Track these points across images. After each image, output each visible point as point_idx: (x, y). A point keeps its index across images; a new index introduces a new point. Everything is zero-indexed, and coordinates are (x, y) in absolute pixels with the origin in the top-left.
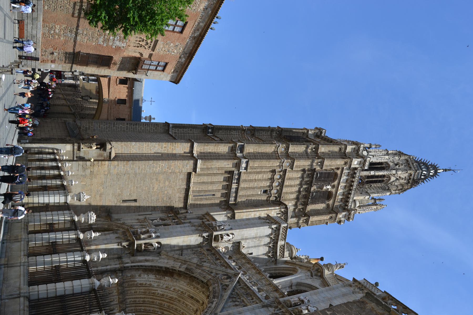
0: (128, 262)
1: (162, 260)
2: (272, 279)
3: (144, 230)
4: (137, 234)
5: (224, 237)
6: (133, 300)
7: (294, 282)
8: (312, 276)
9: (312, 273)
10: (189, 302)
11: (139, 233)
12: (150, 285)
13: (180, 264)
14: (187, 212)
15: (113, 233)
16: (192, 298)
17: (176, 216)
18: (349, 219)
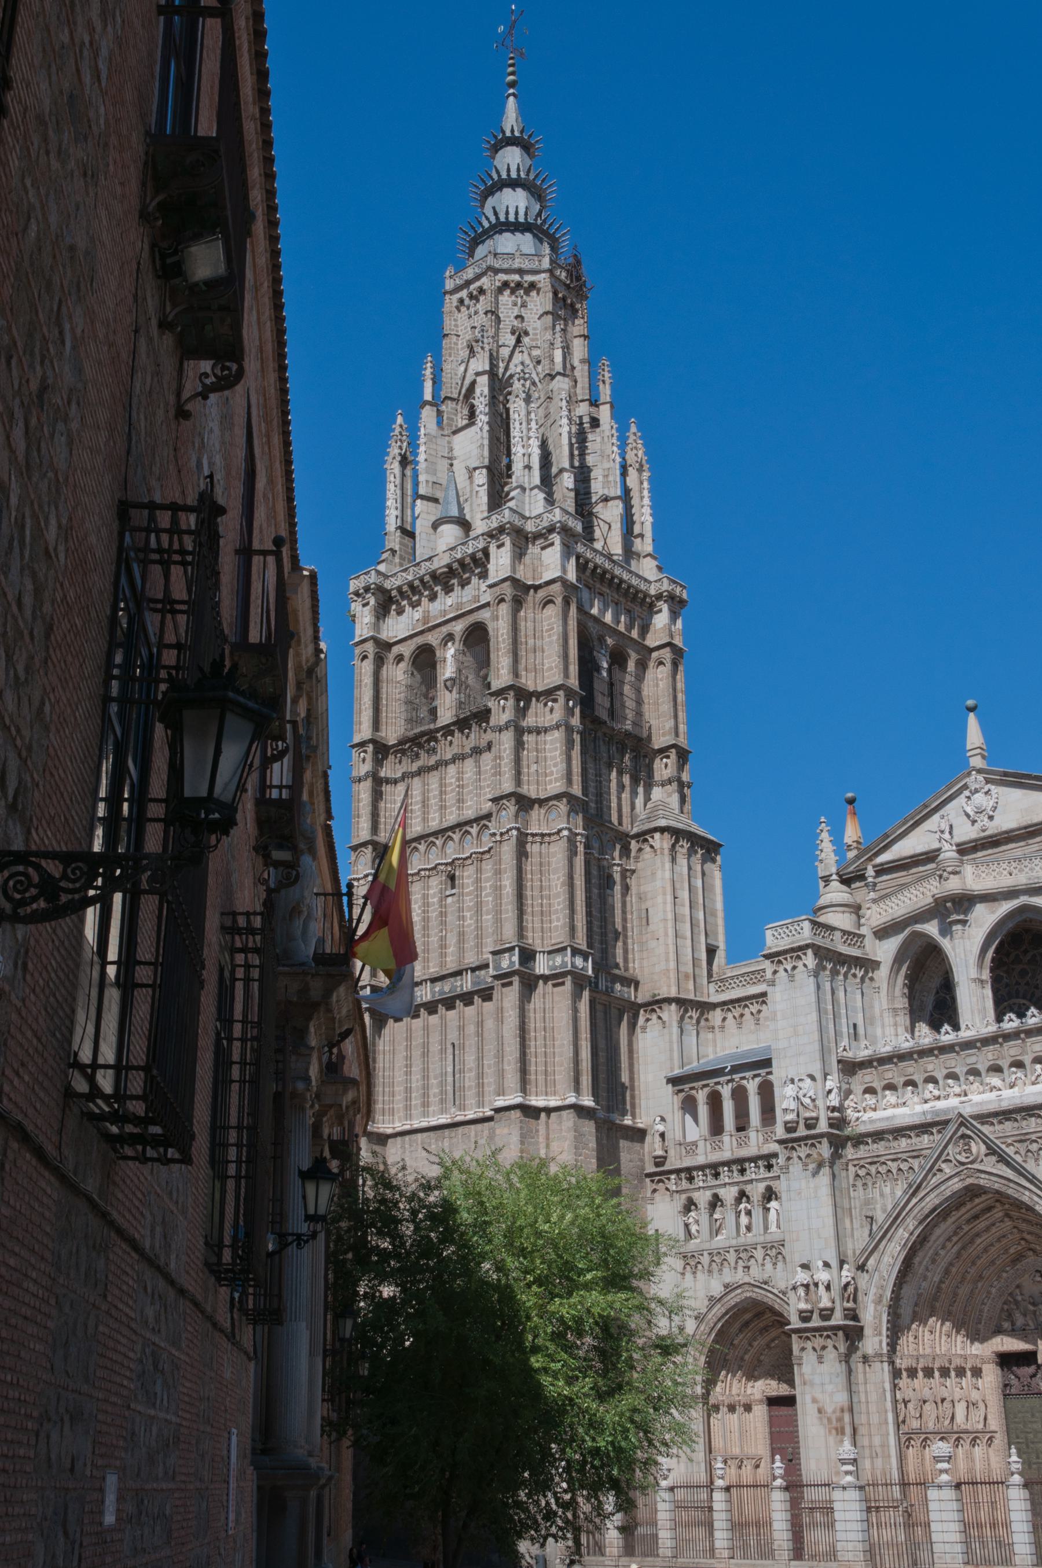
0: (874, 1342)
1: (883, 1267)
2: (963, 1026)
3: (801, 1291)
4: (812, 1312)
5: (833, 1104)
6: (944, 1338)
7: (973, 973)
8: (964, 922)
9: (958, 922)
10: (981, 1224)
11: (809, 1307)
12: (920, 1295)
13: (901, 1230)
14: (662, 1135)
15: (800, 1364)
16: (976, 1217)
17: (678, 1171)
18: (682, 602)
